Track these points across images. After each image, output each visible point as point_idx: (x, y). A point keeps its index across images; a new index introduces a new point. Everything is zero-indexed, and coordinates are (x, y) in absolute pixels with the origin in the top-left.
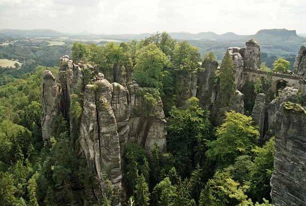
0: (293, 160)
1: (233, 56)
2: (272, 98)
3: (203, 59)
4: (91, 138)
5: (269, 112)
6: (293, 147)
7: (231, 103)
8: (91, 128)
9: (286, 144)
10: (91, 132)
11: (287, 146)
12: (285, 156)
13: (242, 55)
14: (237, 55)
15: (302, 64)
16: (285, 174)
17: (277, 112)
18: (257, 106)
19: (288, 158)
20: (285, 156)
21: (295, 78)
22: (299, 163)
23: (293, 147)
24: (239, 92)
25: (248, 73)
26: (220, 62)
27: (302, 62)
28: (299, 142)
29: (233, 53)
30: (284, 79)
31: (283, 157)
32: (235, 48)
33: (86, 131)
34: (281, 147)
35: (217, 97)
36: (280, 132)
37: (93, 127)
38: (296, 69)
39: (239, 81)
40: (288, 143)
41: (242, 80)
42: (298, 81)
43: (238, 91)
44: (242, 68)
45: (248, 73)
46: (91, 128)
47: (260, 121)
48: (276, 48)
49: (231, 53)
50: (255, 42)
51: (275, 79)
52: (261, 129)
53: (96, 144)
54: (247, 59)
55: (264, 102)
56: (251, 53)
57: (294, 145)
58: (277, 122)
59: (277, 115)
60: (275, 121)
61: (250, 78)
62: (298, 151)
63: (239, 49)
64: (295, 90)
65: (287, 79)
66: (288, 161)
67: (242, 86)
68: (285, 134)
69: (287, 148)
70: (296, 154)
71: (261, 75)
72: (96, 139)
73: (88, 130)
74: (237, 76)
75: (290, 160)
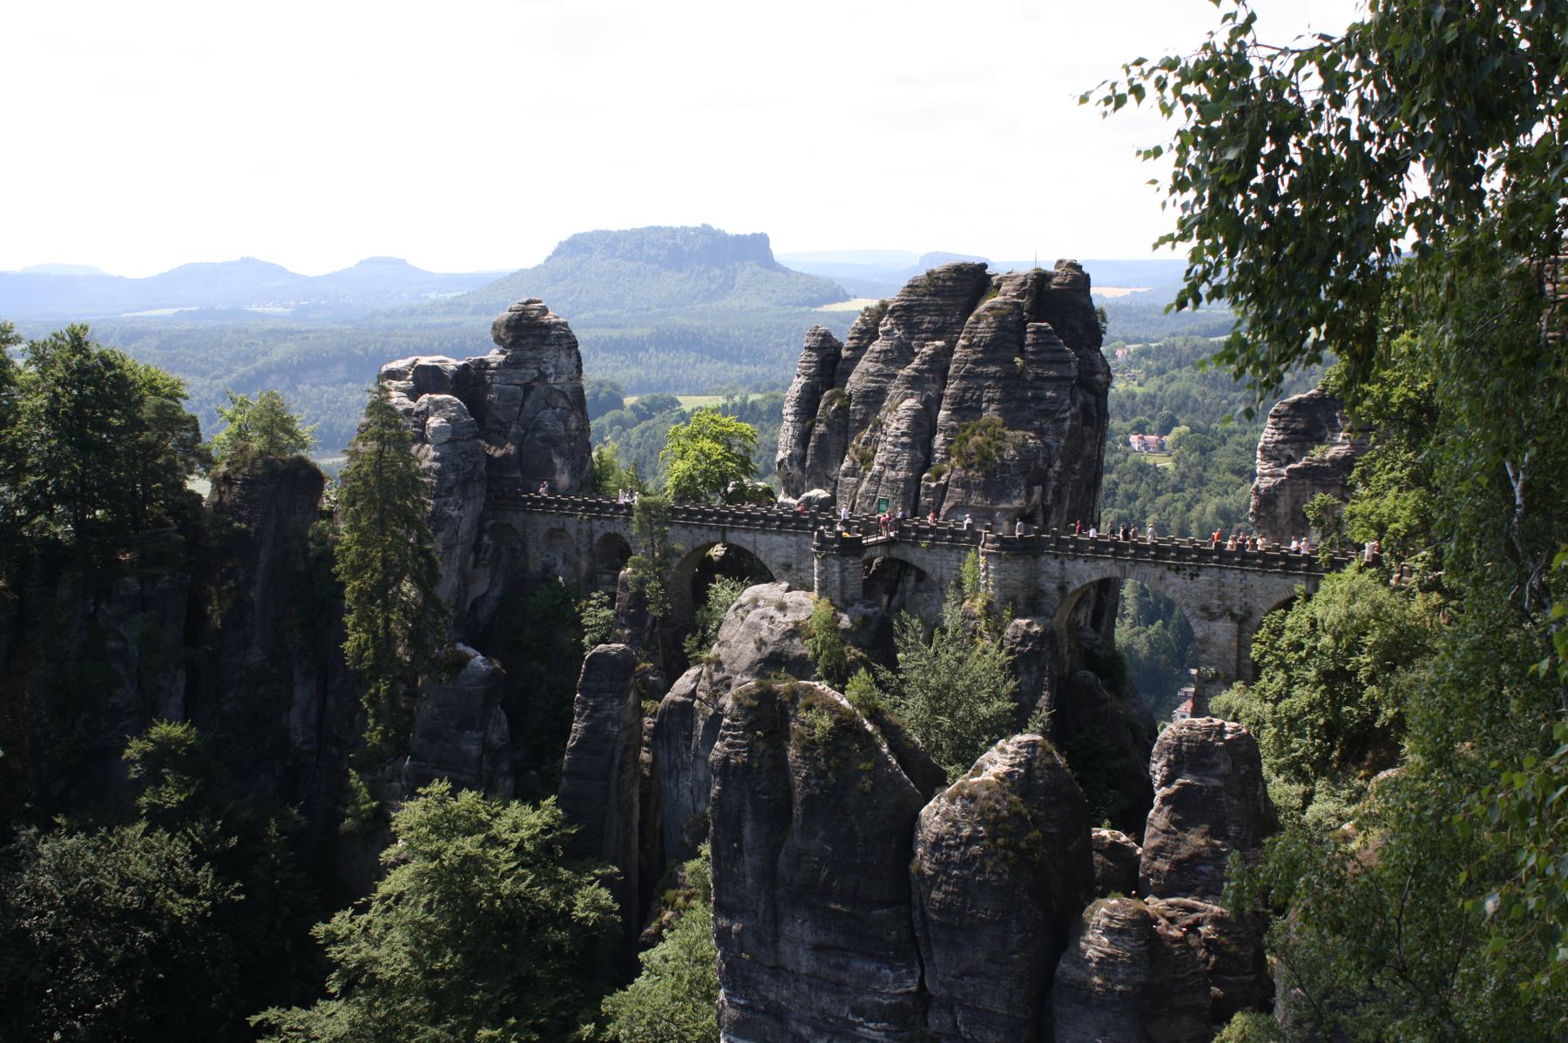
6: (817, 948)
9: (777, 936)
11: (786, 948)
14: (438, 406)
15: (822, 436)
19: (794, 1025)
23: (817, 948)
24: (470, 651)
25: (516, 519)
26: (331, 462)
27: (820, 428)
29: (413, 394)
32: (424, 361)
39: (466, 581)
40: (786, 930)
43: (461, 647)
45: (516, 519)
48: (668, 341)
49: (399, 400)
55: (631, 698)
63: (452, 364)
64: (798, 596)
65: (749, 537)
70: (838, 988)
74: (448, 548)
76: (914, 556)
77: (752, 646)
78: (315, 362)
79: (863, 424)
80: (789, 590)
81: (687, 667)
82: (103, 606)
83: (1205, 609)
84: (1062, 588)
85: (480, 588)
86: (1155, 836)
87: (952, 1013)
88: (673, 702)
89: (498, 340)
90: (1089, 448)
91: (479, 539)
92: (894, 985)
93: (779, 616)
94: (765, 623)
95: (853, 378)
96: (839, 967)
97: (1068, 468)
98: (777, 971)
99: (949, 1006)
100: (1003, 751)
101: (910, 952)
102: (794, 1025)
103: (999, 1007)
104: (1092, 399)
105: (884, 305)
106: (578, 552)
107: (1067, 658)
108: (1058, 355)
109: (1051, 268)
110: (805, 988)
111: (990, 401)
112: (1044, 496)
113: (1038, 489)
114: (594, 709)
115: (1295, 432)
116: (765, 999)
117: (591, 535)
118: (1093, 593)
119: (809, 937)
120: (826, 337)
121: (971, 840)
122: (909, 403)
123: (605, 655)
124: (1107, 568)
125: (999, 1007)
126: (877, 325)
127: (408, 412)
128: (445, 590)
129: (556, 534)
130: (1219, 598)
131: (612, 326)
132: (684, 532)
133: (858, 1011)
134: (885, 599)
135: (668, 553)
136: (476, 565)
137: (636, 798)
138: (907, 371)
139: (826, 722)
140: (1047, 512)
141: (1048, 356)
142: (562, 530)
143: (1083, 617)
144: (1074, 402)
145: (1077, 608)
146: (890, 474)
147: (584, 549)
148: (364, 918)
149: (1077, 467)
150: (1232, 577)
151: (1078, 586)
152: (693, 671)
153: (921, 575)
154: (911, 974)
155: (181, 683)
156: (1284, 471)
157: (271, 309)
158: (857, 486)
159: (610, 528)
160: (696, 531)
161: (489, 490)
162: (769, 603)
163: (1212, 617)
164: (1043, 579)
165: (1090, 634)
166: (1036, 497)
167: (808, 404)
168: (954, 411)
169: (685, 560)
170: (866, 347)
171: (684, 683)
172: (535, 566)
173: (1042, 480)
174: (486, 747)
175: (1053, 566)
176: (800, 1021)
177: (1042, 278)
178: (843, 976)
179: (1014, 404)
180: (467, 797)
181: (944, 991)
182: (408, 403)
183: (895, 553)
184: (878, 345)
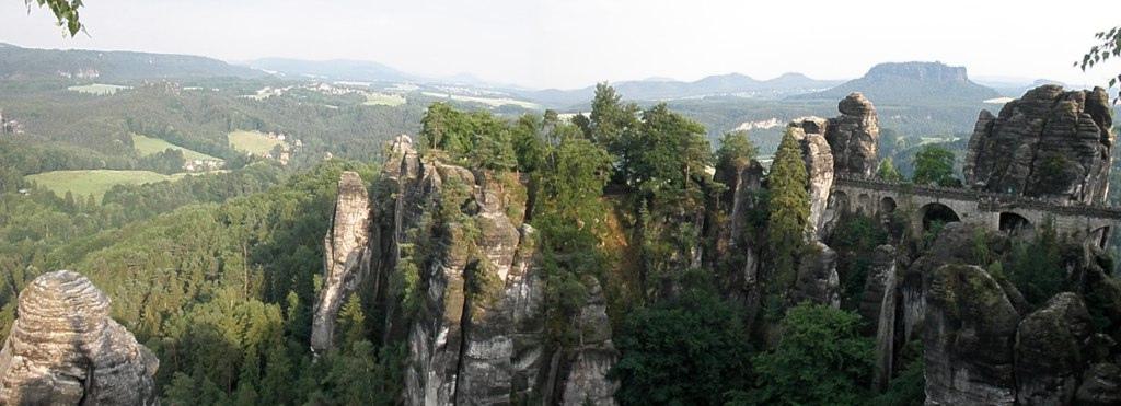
4: (437, 367)
8: (441, 340)
10: (438, 351)
18: (874, 282)
21: (966, 197)
24: (824, 245)
30: (942, 201)
33: (424, 347)
37: (448, 337)
38: (971, 173)
39: (824, 215)
41: (831, 212)
43: (819, 243)
44: (829, 176)
46: (441, 340)
53: (447, 385)
61: (852, 204)
65: (950, 201)
67: (830, 228)
68: (949, 348)
71: (883, 194)
72: (449, 373)
73: (431, 342)
78: (758, 112)
79: (1003, 154)
84: (1088, 230)
90: (1103, 169)
93: (961, 235)
97: (1093, 177)
100: (1058, 299)
112: (1082, 189)
113: (1080, 186)
118: (1101, 231)
121: (1041, 337)
124: (1107, 222)
126: (1011, 110)
134: (1009, 231)
135: (912, 205)
136: (828, 208)
137: (893, 312)
138: (1024, 132)
140: (1083, 197)
143: (1097, 243)
145: (1094, 238)
149: (1098, 177)
151: (1095, 228)
152: (922, 258)
153: (1026, 222)
157: (743, 95)
159: (890, 194)
166: (1079, 190)
171: (917, 263)
173: (1083, 183)
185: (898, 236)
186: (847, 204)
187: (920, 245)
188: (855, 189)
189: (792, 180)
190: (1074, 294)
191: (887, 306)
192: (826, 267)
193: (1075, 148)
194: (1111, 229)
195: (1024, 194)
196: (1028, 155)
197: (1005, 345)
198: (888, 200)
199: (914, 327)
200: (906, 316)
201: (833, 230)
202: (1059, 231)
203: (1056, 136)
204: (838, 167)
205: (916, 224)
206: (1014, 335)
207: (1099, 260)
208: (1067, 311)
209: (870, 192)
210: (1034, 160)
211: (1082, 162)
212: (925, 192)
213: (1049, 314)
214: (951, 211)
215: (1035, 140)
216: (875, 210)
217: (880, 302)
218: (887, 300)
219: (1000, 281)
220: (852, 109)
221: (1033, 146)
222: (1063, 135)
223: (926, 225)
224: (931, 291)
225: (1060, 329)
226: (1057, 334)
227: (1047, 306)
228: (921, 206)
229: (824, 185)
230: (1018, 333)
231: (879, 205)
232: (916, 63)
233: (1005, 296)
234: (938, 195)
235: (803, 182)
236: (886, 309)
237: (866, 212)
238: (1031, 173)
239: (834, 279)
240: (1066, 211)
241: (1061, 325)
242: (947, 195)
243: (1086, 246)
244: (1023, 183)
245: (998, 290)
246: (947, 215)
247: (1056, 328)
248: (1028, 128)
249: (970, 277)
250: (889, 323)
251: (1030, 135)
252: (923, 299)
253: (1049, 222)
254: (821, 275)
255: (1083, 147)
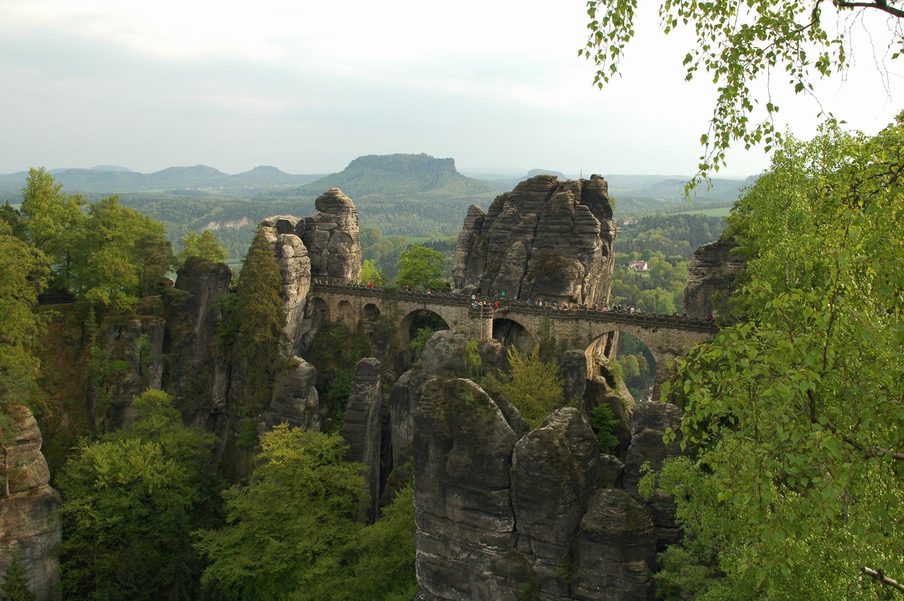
0: (464, 550)
1: (279, 246)
2: (401, 369)
3: (182, 260)
5: (393, 414)
6: (464, 509)
7: (277, 400)
9: (444, 502)
11: (449, 509)
12: (445, 540)
13: (306, 241)
15: (474, 259)
16: (447, 595)
17: (416, 410)
18: (357, 399)
19: (452, 546)
20: (445, 540)
21: (458, 301)
22: (482, 554)
23: (464, 509)
24: (301, 360)
25: (325, 296)
26: (235, 266)
27: (474, 255)
28: (479, 490)
30: (431, 307)
31: (440, 547)
32: (282, 218)
34: (433, 514)
35: (234, 384)
36: (427, 469)
38: (461, 275)
42: (466, 310)
43: (296, 357)
47: (369, 444)
48: (400, 209)
50: (346, 198)
51: (408, 307)
52: (374, 471)
54: (320, 251)
55: (378, 384)
56: (332, 231)
57: (467, 504)
58: (417, 437)
59: (415, 419)
60: (411, 438)
61: (332, 311)
62: (478, 519)
65: (438, 307)
66: (453, 553)
67: (308, 340)
69: (449, 515)
71: (365, 301)
75: (458, 549)
76: (518, 318)
77: (437, 360)
80: (456, 333)
81: (406, 370)
82: (123, 333)
83: (660, 348)
85: (306, 329)
86: (631, 458)
87: (529, 543)
88: (398, 387)
89: (318, 208)
91: (306, 305)
92: (502, 528)
94: (444, 350)
95: (490, 230)
96: (475, 519)
98: (444, 519)
99: (529, 537)
100: (557, 415)
101: (511, 512)
102: (452, 546)
103: (552, 539)
104: (607, 244)
105: (506, 195)
106: (354, 313)
107: (592, 370)
108: (590, 222)
109: (589, 179)
110: (457, 528)
111: (557, 243)
113: (580, 287)
114: (361, 389)
115: (707, 262)
116: (438, 533)
117: (361, 305)
118: (605, 338)
119: (460, 504)
120: (477, 210)
122: (518, 243)
123: (364, 363)
125: (552, 539)
127: (273, 243)
128: (289, 329)
129: (343, 303)
130: (667, 342)
131: (376, 202)
132: (406, 304)
133: (483, 543)
134: (503, 339)
136: (305, 317)
138: (516, 228)
139: (469, 398)
140: (583, 299)
141: (586, 222)
142: (347, 302)
143: (601, 349)
144: (598, 245)
146: (508, 278)
147: (357, 311)
148: (245, 489)
150: (674, 333)
152: (409, 372)
153: (520, 328)
154: (509, 523)
155: (160, 371)
156: (700, 280)
158: (491, 283)
160: (412, 303)
161: (312, 281)
162: (446, 339)
163: (663, 353)
164: (580, 331)
165: (604, 358)
166: (578, 291)
167: (469, 243)
168: (539, 248)
169: (407, 317)
170: (496, 216)
171: (405, 377)
172: (333, 319)
173: (583, 283)
174: (308, 408)
175: (585, 324)
176: (455, 544)
177: (585, 183)
178: (476, 523)
179: (568, 245)
180: (296, 430)
181: (524, 532)
182: (273, 238)
183: (510, 316)
184: (502, 215)
185: (382, 347)
186: (325, 311)
187: (407, 358)
188: (335, 295)
189: (264, 286)
190: (575, 409)
191: (372, 427)
192: (304, 384)
193: (573, 244)
194: (617, 334)
195: (519, 298)
196: (522, 255)
197: (500, 467)
198: (370, 307)
199: (402, 449)
200: (394, 439)
201: (312, 343)
202: (557, 337)
203: (551, 231)
204: (316, 271)
205: (401, 335)
206: (511, 457)
207: (604, 371)
208: (568, 428)
209: (352, 299)
210: (529, 256)
211: (581, 260)
212: (411, 297)
213: (549, 432)
214: (439, 318)
215: (529, 237)
216: (357, 319)
217: (365, 422)
218: (373, 419)
219: (495, 396)
220: (330, 204)
221: (526, 243)
222: (559, 231)
223: (413, 335)
224: (418, 408)
225: (560, 450)
226: (558, 454)
227: (545, 424)
228: (406, 314)
229: (298, 293)
230: (514, 455)
231: (360, 313)
232: (401, 155)
233: (499, 413)
234: (426, 300)
235: (277, 289)
236: (372, 430)
237: (347, 321)
238: (525, 273)
239: (313, 398)
240: (564, 316)
241: (562, 445)
242: (435, 300)
243: (588, 353)
244: (516, 284)
245: (492, 406)
246: (437, 323)
247: (556, 447)
248: (521, 224)
249: (462, 391)
250: (375, 446)
251: (522, 232)
252: (411, 418)
253: (547, 328)
254: (298, 395)
255: (581, 243)
